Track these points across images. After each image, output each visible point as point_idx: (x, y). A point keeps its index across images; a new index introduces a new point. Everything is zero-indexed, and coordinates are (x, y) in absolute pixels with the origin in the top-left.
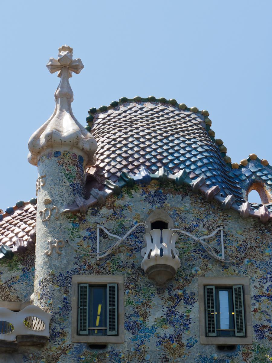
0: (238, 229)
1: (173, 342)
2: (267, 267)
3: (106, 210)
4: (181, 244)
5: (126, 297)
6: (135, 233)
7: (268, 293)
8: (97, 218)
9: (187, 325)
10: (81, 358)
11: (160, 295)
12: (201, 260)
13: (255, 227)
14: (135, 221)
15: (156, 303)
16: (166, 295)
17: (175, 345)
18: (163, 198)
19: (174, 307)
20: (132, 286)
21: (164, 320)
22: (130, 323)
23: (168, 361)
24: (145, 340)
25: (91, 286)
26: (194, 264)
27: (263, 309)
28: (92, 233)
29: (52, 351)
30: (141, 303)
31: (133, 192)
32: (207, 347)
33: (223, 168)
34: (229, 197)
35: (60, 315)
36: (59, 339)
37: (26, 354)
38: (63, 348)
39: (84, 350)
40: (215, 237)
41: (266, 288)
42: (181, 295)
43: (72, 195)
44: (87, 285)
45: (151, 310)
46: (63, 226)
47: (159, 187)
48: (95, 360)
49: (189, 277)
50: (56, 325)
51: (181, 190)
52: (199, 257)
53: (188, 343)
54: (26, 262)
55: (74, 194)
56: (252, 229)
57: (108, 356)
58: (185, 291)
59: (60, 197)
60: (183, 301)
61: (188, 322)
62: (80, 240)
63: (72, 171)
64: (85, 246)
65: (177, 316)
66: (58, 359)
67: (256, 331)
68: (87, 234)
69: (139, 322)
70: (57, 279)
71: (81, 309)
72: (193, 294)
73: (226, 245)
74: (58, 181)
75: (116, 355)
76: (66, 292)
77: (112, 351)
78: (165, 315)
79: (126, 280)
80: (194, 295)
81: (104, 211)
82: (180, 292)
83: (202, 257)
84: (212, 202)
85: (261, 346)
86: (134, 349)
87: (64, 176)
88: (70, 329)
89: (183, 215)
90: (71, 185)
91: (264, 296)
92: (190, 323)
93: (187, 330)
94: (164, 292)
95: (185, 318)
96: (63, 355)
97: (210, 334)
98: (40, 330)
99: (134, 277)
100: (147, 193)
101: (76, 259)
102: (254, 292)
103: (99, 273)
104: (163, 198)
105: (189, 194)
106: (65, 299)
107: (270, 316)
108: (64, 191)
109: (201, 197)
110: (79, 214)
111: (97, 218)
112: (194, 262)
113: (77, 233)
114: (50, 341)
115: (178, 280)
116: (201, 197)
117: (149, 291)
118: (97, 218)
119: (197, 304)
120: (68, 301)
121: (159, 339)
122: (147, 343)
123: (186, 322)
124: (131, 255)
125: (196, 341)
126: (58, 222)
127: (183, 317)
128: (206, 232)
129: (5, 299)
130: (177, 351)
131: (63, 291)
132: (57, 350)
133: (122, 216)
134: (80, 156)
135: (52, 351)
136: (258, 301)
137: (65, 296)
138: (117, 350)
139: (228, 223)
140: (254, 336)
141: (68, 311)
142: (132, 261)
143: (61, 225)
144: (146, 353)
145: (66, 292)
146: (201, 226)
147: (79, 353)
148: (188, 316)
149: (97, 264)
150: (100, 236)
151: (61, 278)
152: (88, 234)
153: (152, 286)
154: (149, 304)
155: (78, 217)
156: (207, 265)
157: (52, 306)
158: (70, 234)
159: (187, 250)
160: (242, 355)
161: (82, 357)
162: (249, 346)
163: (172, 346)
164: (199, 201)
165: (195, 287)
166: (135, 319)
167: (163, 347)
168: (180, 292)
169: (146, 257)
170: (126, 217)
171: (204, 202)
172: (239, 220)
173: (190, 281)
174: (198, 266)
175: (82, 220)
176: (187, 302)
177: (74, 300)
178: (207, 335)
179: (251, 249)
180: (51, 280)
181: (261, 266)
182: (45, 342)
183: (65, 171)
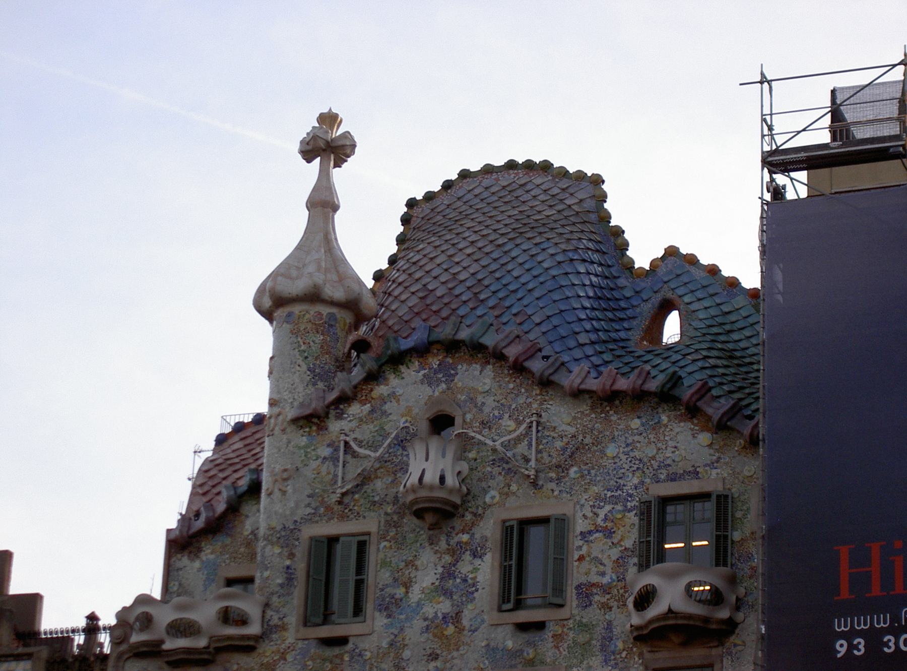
0: (564, 416)
1: (447, 626)
4: (474, 452)
5: (381, 555)
9: (472, 593)
12: (501, 478)
13: (593, 408)
14: (403, 420)
15: (425, 562)
16: (443, 545)
17: (451, 630)
18: (452, 372)
19: (454, 565)
20: (391, 534)
21: (436, 590)
27: (594, 554)
29: (267, 657)
30: (403, 564)
31: (403, 368)
32: (500, 629)
35: (279, 596)
37: (228, 665)
38: (282, 651)
39: (313, 651)
40: (527, 434)
41: (602, 516)
42: (466, 543)
43: (310, 387)
45: (419, 573)
49: (480, 511)
50: (272, 613)
52: (500, 473)
55: (314, 384)
57: (346, 658)
60: (468, 552)
63: (312, 343)
64: (324, 473)
67: (578, 594)
68: (326, 452)
69: (397, 596)
73: (541, 447)
76: (291, 556)
79: (382, 523)
81: (355, 409)
82: (465, 538)
85: (584, 621)
87: (298, 357)
88: (293, 619)
89: (480, 399)
92: (477, 590)
94: (439, 540)
99: (395, 518)
100: (427, 366)
101: (309, 496)
102: (581, 525)
103: (343, 517)
104: (452, 372)
106: (288, 567)
107: (605, 566)
108: (297, 381)
110: (315, 420)
111: (343, 424)
112: (491, 483)
113: (313, 453)
115: (463, 516)
117: (417, 541)
119: (488, 558)
121: (426, 623)
123: (470, 587)
124: (393, 482)
125: (483, 621)
126: (285, 437)
127: (466, 581)
128: (512, 425)
130: (453, 641)
131: (286, 554)
133: (384, 413)
136: (587, 541)
137: (288, 562)
138: (362, 646)
140: (575, 603)
142: (395, 490)
143: (289, 442)
145: (291, 556)
146: (507, 416)
148: (474, 578)
150: (346, 452)
151: (283, 533)
153: (422, 532)
156: (509, 486)
160: (551, 640)
161: (308, 663)
162: (565, 622)
163: (445, 633)
164: (506, 372)
165: (489, 529)
171: (513, 373)
173: (481, 516)
176: (475, 555)
177: (301, 567)
179: (583, 448)
181: (598, 478)
183: (300, 346)
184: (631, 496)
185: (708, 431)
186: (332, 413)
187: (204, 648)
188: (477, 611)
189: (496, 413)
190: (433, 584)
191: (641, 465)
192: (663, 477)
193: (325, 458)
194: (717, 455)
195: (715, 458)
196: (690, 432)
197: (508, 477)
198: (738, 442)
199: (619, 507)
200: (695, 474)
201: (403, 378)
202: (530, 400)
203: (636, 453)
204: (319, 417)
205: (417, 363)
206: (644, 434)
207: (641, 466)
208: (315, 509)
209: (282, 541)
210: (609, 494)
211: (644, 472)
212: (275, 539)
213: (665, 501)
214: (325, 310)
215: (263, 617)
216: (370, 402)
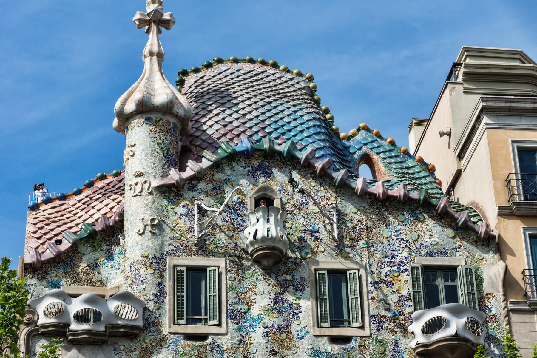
2: (385, 250)
3: (205, 184)
6: (237, 210)
7: (386, 279)
8: (194, 194)
9: (297, 314)
10: (178, 351)
11: (267, 280)
13: (371, 205)
18: (269, 171)
19: (283, 294)
22: (233, 312)
23: (276, 354)
24: (250, 330)
25: (190, 269)
26: (303, 246)
28: (189, 210)
31: (234, 164)
32: (320, 339)
33: (331, 139)
34: (343, 172)
35: (154, 302)
36: (154, 329)
37: (116, 346)
38: (158, 339)
42: (289, 281)
44: (184, 269)
46: (157, 202)
47: (263, 159)
48: (195, 353)
51: (288, 163)
52: (310, 238)
53: (298, 334)
54: (112, 242)
56: (368, 207)
57: (208, 348)
58: (293, 276)
59: (152, 169)
60: (292, 287)
61: (298, 311)
62: (176, 218)
63: (165, 140)
65: (286, 305)
66: (153, 352)
69: (243, 311)
70: (151, 261)
71: (178, 296)
72: (303, 279)
74: (150, 152)
75: (219, 347)
76: (162, 276)
77: (214, 343)
78: (273, 303)
80: (305, 280)
81: (202, 185)
82: (289, 277)
83: (312, 239)
84: (324, 177)
85: (379, 338)
86: (238, 341)
87: (156, 146)
90: (164, 156)
91: (382, 282)
93: (297, 319)
95: (295, 306)
96: (158, 347)
97: (324, 325)
98: (133, 318)
100: (250, 165)
104: (269, 171)
105: (297, 167)
106: (160, 284)
109: (311, 171)
110: (174, 189)
114: (143, 332)
115: (286, 263)
116: (311, 171)
118: (194, 194)
120: (163, 287)
122: (252, 334)
125: (308, 332)
126: (151, 197)
129: (87, 284)
130: (286, 344)
132: (151, 342)
134: (173, 123)
135: (146, 343)
137: (160, 280)
138: (219, 341)
139: (341, 200)
140: (372, 326)
141: (163, 298)
144: (252, 345)
147: (176, 345)
149: (195, 246)
150: (199, 213)
152: (185, 212)
153: (258, 270)
154: (255, 290)
155: (173, 192)
156: (318, 248)
157: (146, 292)
158: (165, 211)
159: (296, 230)
160: (358, 349)
161: (179, 349)
166: (239, 307)
167: (270, 338)
168: (289, 277)
169: (251, 238)
170: (227, 192)
171: (315, 177)
172: (354, 197)
173: (300, 265)
174: (308, 248)
175: (177, 196)
177: (168, 285)
178: (320, 326)
180: (144, 262)
181: (379, 250)
182: (138, 332)
184: (403, 263)
185: (452, 228)
186: (187, 186)
187: (103, 331)
188: (302, 326)
189: (304, 200)
190: (269, 305)
191: (408, 244)
192: (423, 253)
193: (181, 215)
194: (458, 243)
195: (457, 245)
196: (441, 228)
197: (316, 242)
198: (472, 237)
199: (395, 268)
200: (445, 254)
201: (234, 170)
202: (327, 195)
203: (404, 237)
204: (176, 188)
205: (243, 163)
206: (408, 225)
207: (408, 245)
208: (177, 247)
209: (154, 265)
210: (387, 260)
211: (410, 249)
212: (148, 264)
213: (426, 269)
214: (172, 120)
215: (143, 315)
216: (212, 183)
